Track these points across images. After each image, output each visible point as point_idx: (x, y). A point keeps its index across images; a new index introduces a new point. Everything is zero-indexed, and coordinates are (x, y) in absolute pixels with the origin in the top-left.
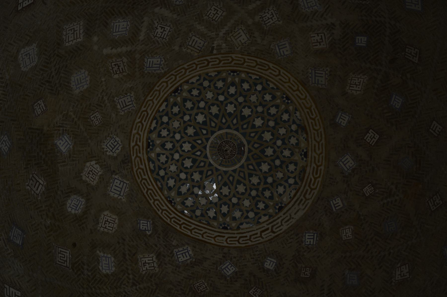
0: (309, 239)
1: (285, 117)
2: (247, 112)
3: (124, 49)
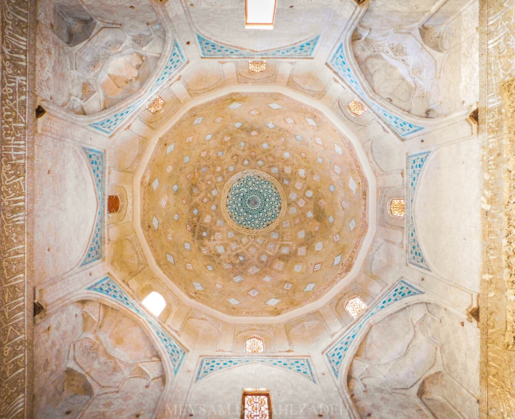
0: (231, 169)
1: (232, 211)
2: (245, 214)
3: (285, 243)
